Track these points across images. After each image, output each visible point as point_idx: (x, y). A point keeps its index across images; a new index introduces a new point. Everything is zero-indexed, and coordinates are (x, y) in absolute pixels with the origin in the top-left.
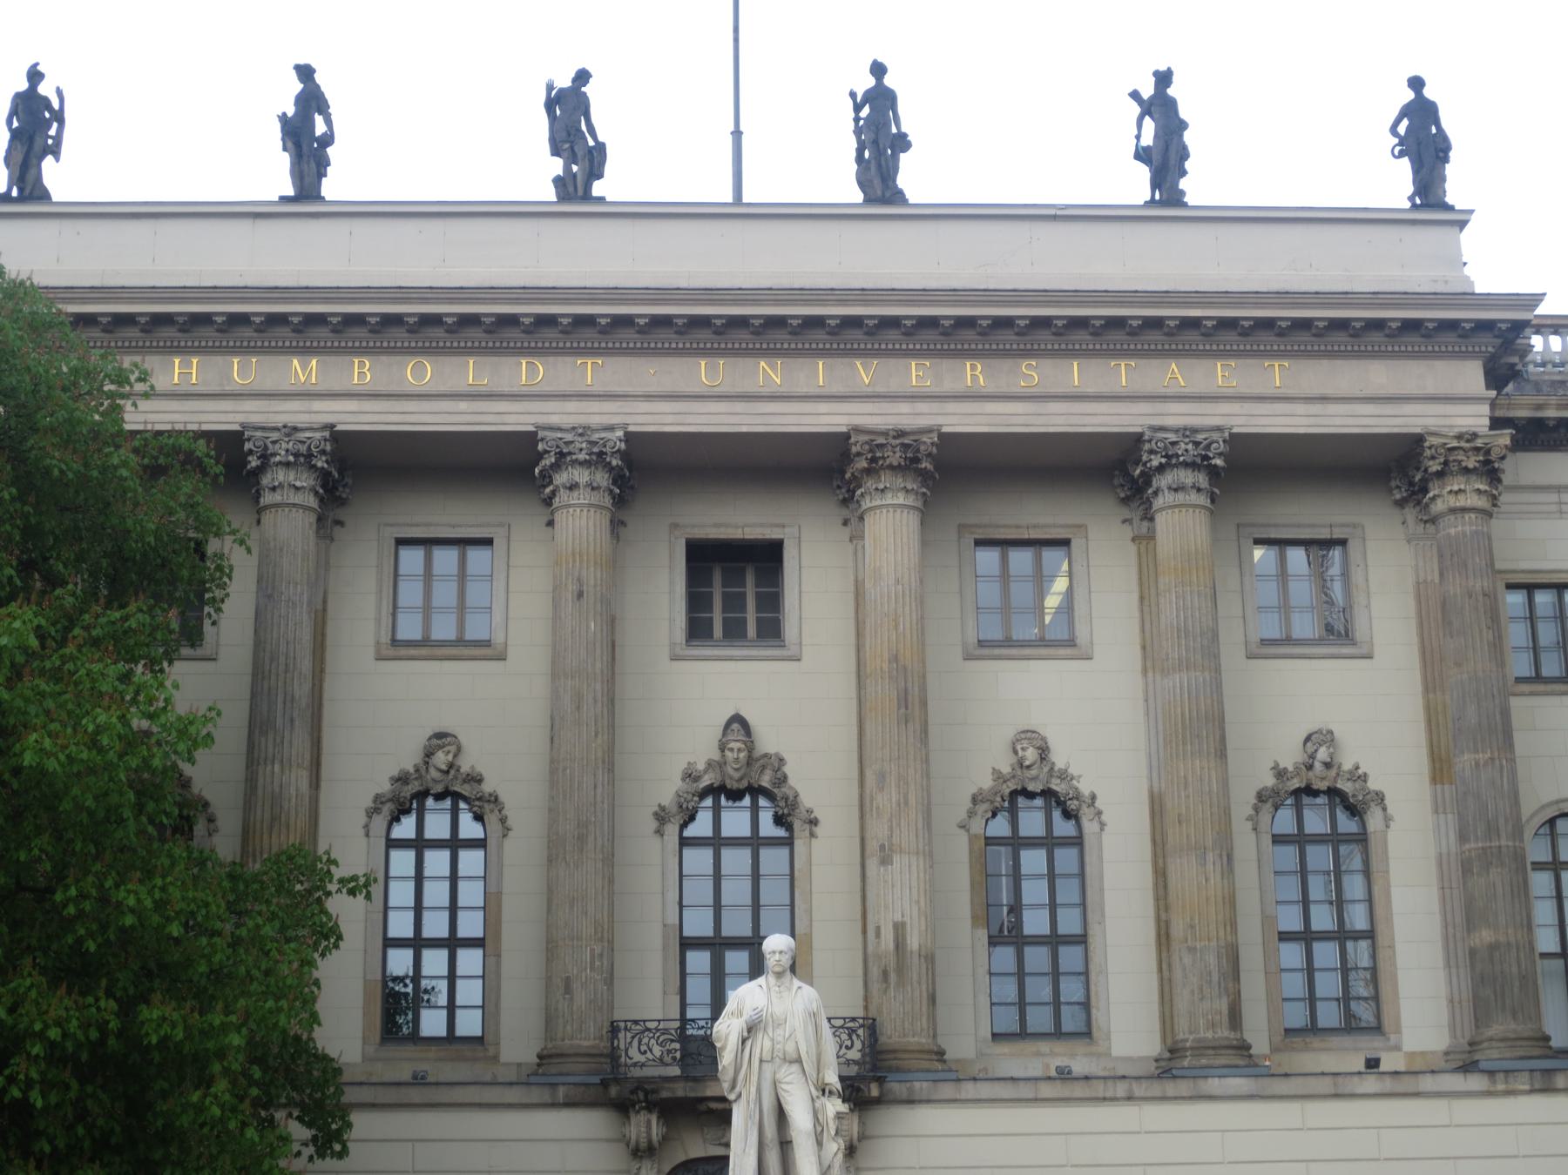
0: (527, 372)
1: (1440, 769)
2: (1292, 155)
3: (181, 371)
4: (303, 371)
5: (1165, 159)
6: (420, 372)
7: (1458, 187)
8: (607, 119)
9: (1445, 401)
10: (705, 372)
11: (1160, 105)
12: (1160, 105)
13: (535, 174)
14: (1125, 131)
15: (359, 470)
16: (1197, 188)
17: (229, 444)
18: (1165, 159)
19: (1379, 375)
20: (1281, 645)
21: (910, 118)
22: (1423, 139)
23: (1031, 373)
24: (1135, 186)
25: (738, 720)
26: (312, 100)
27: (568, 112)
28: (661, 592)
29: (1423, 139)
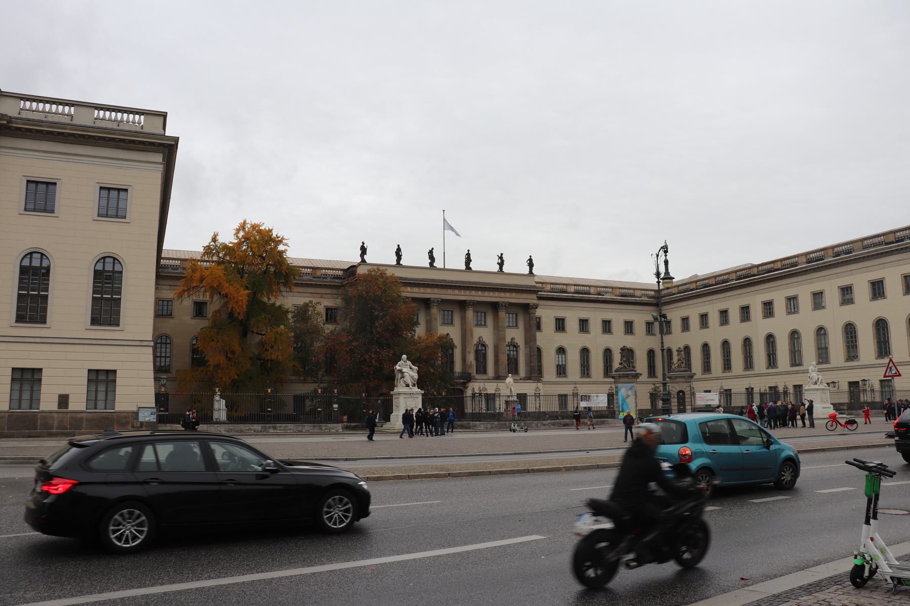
0: (429, 290)
1: (526, 343)
2: (516, 266)
5: (501, 264)
6: (416, 289)
7: (534, 271)
9: (531, 299)
10: (450, 291)
11: (501, 258)
13: (426, 263)
14: (497, 260)
16: (505, 269)
18: (501, 264)
19: (525, 296)
20: (509, 327)
22: (531, 265)
23: (486, 293)
24: (497, 268)
29: (531, 265)
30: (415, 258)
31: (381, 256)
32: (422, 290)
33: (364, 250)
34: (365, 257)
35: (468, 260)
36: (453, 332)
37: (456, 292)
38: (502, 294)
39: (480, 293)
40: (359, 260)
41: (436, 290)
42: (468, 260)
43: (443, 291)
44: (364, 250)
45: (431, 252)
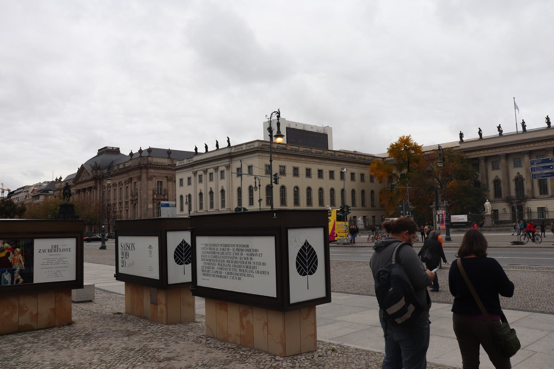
0: (498, 150)
3: (474, 153)
4: (482, 152)
6: (490, 151)
8: (503, 128)
10: (511, 148)
11: (548, 118)
12: (548, 118)
13: (497, 133)
15: (486, 158)
17: (477, 158)
21: (526, 124)
23: (536, 144)
24: (546, 125)
25: (518, 173)
26: (480, 130)
27: (499, 127)
28: (511, 164)
30: (490, 132)
31: (471, 135)
32: (494, 151)
33: (461, 135)
34: (463, 139)
35: (524, 126)
36: (522, 171)
37: (516, 147)
38: (549, 143)
39: (532, 145)
40: (459, 140)
41: (502, 149)
42: (524, 126)
43: (507, 149)
44: (461, 135)
45: (499, 127)
